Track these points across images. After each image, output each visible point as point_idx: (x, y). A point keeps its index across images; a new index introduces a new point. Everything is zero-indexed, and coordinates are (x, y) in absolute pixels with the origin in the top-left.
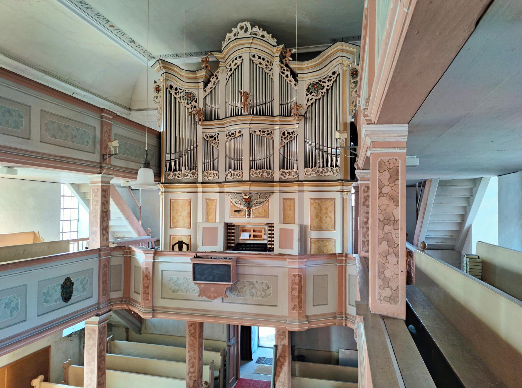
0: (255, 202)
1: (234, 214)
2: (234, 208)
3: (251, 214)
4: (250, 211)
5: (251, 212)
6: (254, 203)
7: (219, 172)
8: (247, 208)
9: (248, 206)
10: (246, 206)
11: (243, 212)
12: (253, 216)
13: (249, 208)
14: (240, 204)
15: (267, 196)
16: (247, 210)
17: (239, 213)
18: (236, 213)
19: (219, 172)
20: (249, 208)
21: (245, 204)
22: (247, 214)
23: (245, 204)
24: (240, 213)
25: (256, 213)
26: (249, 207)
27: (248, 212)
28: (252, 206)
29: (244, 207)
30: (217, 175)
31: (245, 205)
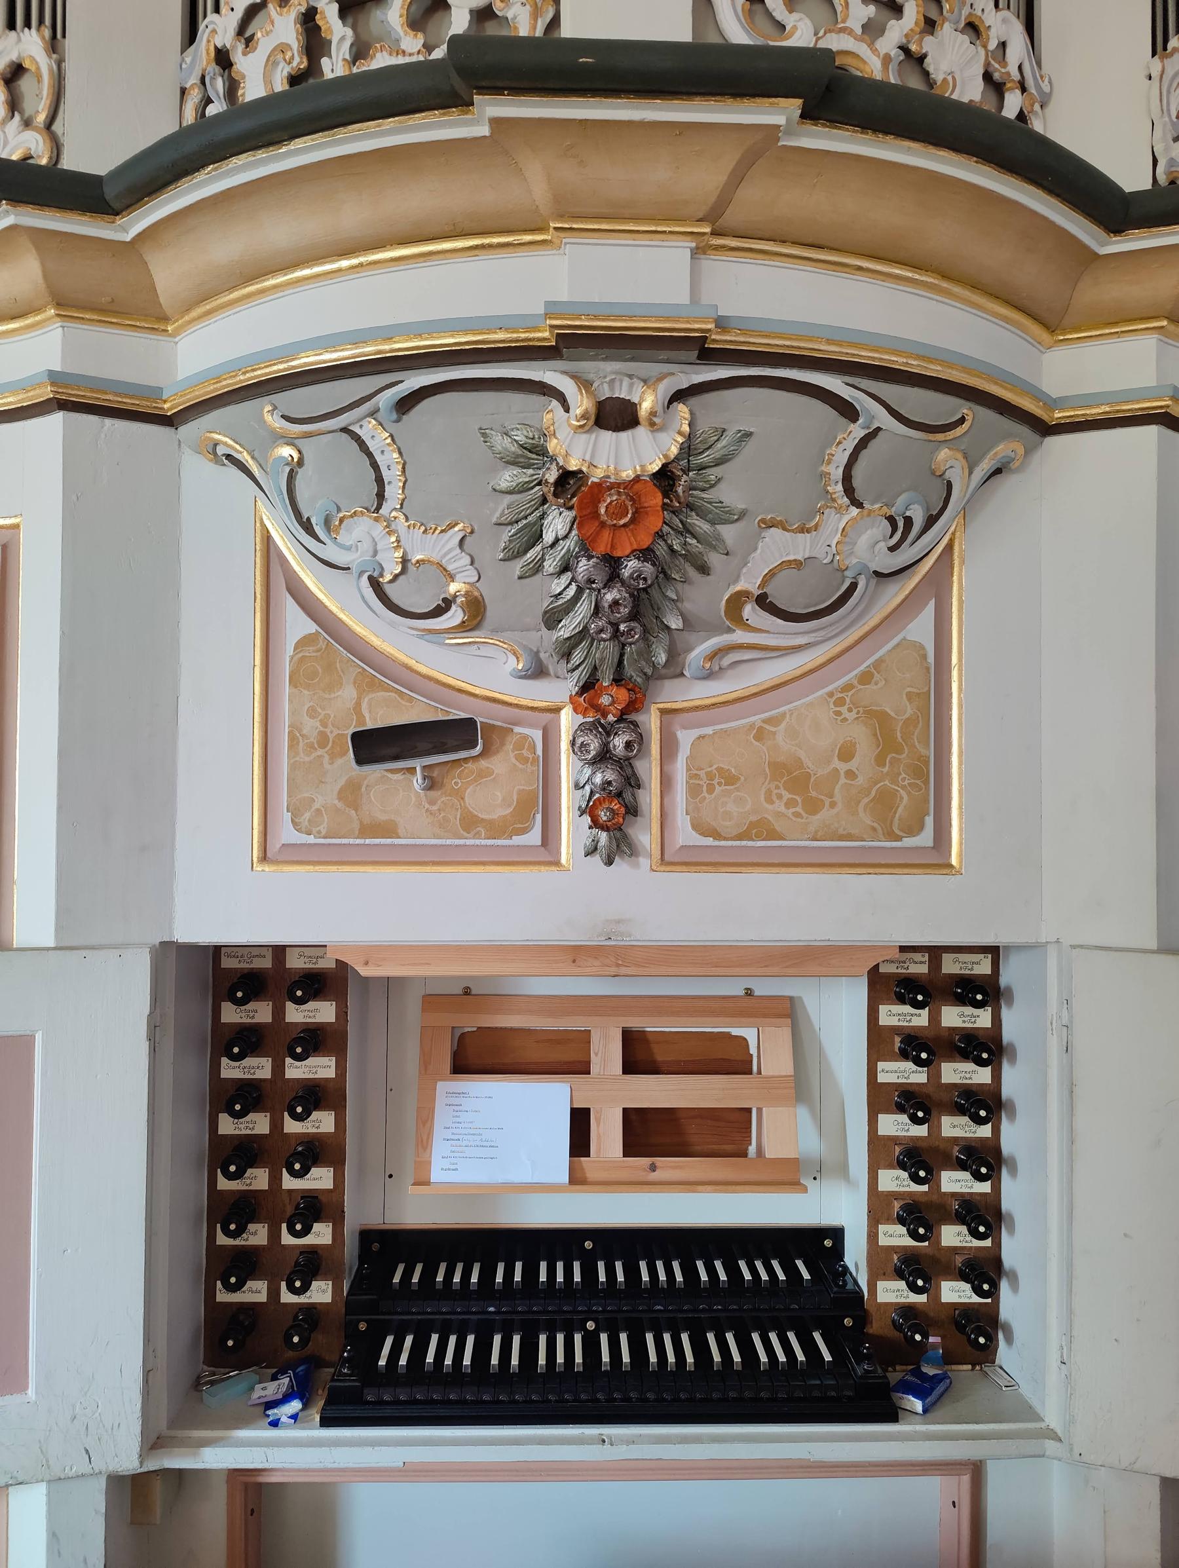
0: (750, 582)
1: (351, 794)
2: (348, 693)
3: (650, 798)
4: (638, 742)
5: (649, 769)
6: (736, 603)
7: (54, 45)
8: (588, 687)
9: (606, 651)
10: (566, 650)
11: (500, 764)
12: (684, 834)
13: (610, 698)
14: (455, 616)
15: (956, 476)
16: (568, 720)
17: (431, 784)
18: (375, 771)
19: (71, 44)
20: (610, 698)
21: (552, 619)
22: (568, 801)
23: (552, 619)
24: (454, 781)
25: (730, 780)
26: (619, 680)
27: (604, 757)
28: (674, 668)
29: (538, 671)
30: (28, 105)
31: (568, 627)
